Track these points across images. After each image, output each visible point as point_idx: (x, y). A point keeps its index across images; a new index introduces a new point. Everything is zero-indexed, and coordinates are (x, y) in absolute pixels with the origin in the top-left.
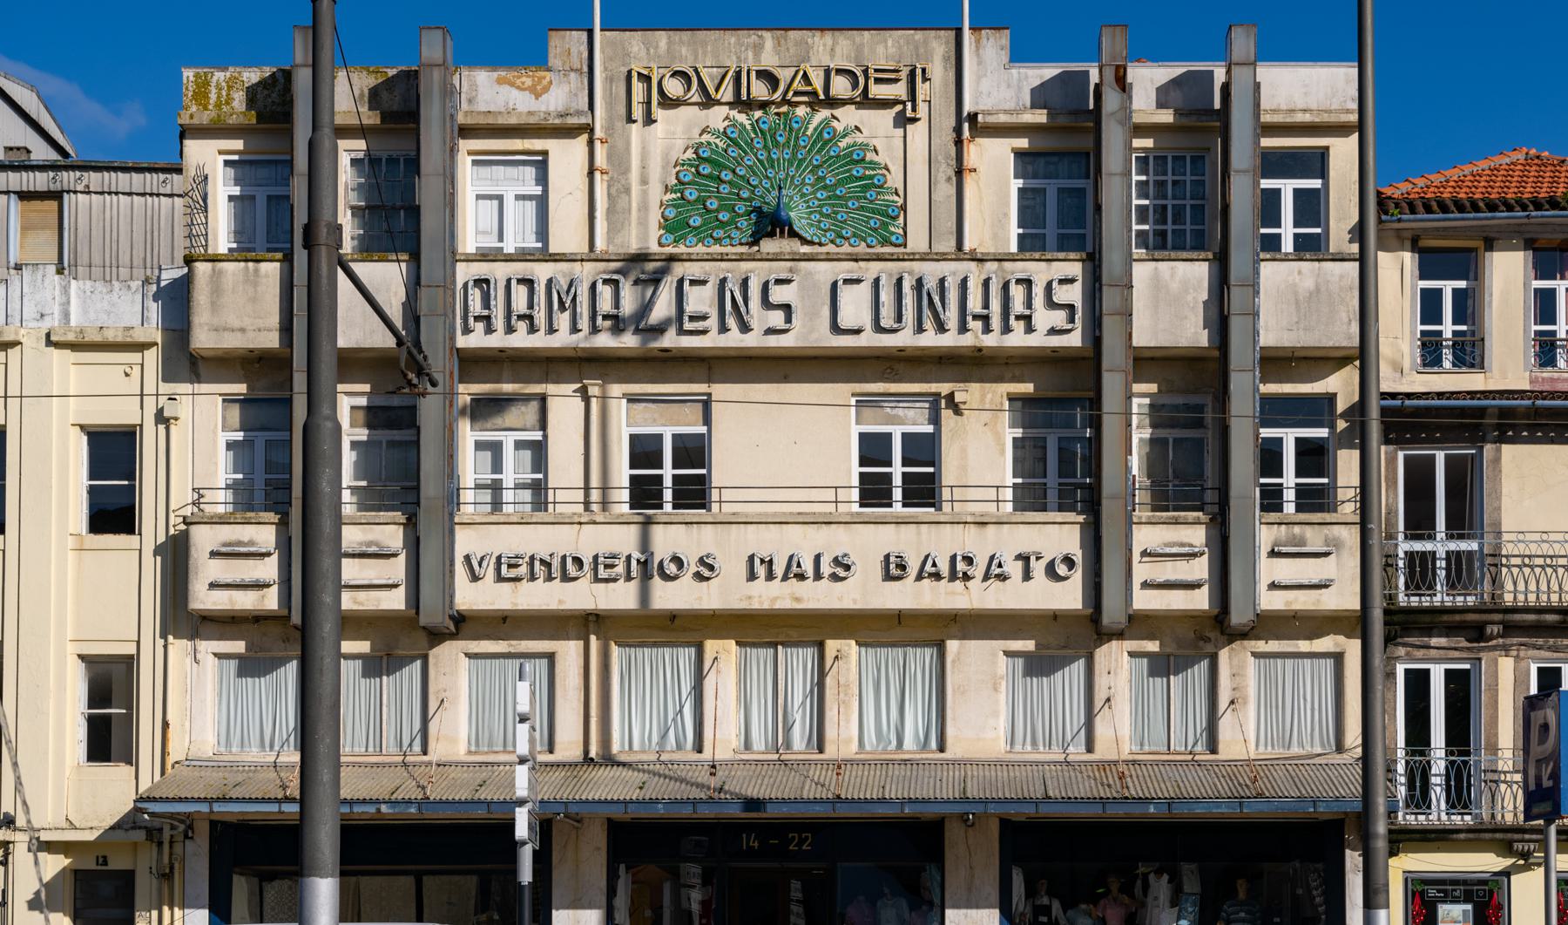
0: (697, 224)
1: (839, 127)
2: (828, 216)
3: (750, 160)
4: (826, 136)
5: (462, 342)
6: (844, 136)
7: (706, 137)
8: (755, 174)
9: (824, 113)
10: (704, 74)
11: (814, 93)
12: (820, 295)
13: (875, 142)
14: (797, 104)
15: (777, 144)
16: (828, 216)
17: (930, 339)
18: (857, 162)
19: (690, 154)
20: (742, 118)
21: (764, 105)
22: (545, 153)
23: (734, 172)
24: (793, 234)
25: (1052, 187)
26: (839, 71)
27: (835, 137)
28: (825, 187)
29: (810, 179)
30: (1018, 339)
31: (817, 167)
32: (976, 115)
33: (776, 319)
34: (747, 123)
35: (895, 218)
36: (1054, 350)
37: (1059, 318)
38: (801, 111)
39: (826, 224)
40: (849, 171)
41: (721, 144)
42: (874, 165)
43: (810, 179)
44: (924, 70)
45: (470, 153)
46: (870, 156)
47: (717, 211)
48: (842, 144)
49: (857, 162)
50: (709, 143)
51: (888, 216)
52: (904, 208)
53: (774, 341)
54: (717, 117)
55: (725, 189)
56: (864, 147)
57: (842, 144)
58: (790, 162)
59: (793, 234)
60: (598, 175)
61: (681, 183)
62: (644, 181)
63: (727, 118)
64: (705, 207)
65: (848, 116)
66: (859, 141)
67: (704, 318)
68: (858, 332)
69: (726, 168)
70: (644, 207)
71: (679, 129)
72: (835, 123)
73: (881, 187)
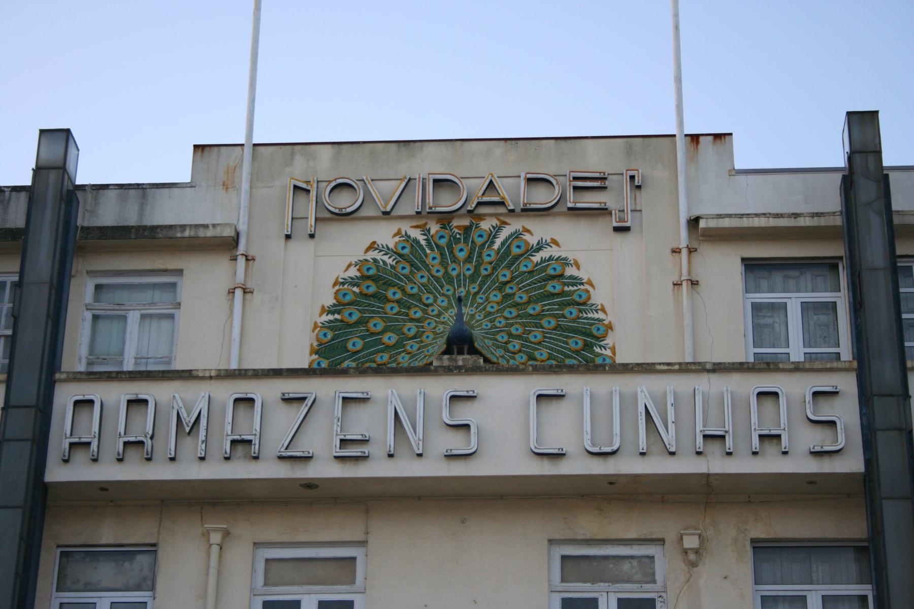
1: (532, 240)
2: (518, 337)
3: (422, 277)
4: (515, 251)
5: (56, 473)
6: (538, 250)
9: (515, 225)
11: (502, 204)
12: (509, 422)
14: (481, 217)
15: (455, 260)
16: (518, 337)
18: (553, 277)
20: (416, 234)
21: (445, 218)
22: (179, 272)
23: (403, 290)
24: (474, 351)
25: (794, 301)
26: (530, 180)
28: (516, 305)
33: (456, 443)
34: (422, 239)
36: (811, 480)
37: (816, 438)
38: (486, 225)
41: (390, 261)
42: (576, 281)
45: (91, 273)
46: (570, 271)
47: (382, 332)
48: (536, 258)
49: (553, 277)
50: (375, 260)
51: (594, 337)
52: (610, 327)
57: (536, 258)
58: (473, 279)
59: (474, 351)
63: (398, 233)
65: (538, 231)
67: (364, 441)
72: (527, 237)
73: (584, 304)
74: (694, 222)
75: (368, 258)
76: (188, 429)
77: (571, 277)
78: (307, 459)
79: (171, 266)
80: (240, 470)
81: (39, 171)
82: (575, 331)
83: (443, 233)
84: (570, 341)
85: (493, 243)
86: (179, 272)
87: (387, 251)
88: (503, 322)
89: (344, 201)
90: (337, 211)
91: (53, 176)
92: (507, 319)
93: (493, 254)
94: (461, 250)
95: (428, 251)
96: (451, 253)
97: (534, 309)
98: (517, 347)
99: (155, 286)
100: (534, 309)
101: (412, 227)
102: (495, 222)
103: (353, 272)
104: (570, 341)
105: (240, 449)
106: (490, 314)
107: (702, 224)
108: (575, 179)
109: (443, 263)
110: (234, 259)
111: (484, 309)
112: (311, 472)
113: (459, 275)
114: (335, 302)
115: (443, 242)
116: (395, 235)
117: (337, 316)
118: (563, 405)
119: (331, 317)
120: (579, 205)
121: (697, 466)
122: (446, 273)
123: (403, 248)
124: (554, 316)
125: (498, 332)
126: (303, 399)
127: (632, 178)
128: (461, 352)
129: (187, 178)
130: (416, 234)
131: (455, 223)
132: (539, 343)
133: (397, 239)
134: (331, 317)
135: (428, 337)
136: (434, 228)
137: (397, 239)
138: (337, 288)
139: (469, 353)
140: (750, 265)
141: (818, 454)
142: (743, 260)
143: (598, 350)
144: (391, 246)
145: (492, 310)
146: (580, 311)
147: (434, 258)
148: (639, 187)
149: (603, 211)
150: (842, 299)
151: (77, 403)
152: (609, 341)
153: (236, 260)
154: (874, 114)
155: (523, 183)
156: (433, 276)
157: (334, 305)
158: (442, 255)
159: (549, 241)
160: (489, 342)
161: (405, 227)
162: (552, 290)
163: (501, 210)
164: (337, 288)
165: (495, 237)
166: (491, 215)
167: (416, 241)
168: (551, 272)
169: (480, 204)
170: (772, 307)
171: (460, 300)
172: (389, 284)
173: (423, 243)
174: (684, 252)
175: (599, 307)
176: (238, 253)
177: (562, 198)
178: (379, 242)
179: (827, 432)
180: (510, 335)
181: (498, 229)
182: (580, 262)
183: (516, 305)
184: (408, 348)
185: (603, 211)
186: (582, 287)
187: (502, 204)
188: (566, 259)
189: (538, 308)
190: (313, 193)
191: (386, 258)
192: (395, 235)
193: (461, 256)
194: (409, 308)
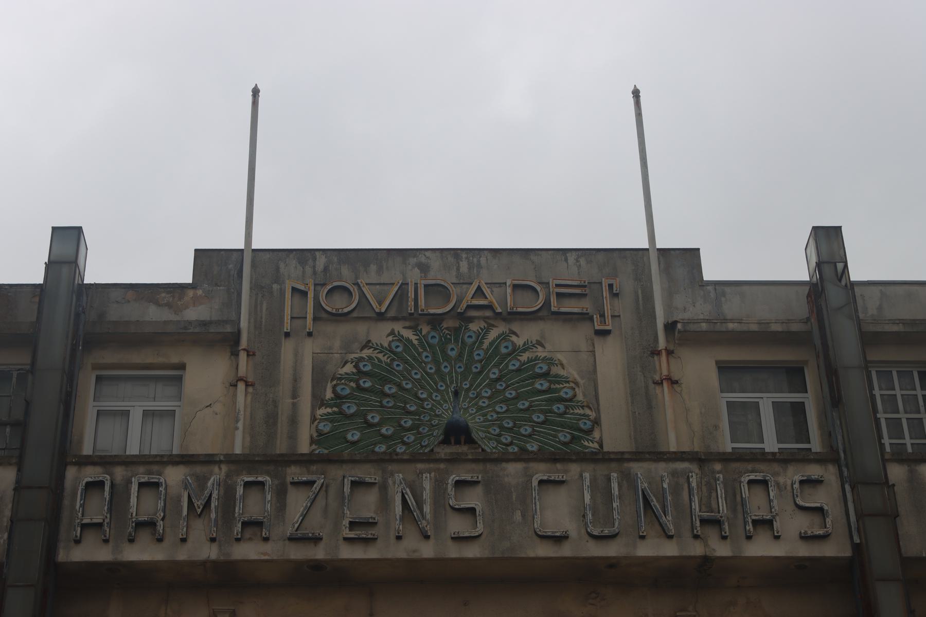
0: (356, 438)
1: (519, 342)
4: (504, 351)
6: (524, 351)
7: (366, 353)
8: (423, 388)
10: (366, 290)
13: (559, 356)
14: (471, 320)
15: (446, 358)
17: (652, 548)
19: (349, 368)
20: (408, 334)
21: (435, 321)
23: (399, 386)
25: (766, 403)
26: (515, 287)
27: (515, 351)
28: (506, 401)
29: (487, 393)
30: (761, 548)
31: (498, 380)
32: (675, 323)
34: (413, 338)
35: (589, 432)
38: (474, 327)
39: (506, 438)
40: (533, 384)
41: (384, 359)
43: (487, 393)
44: (611, 286)
45: (96, 367)
46: (555, 370)
47: (379, 424)
48: (524, 357)
50: (370, 358)
51: (581, 430)
52: (597, 422)
53: (454, 552)
54: (381, 334)
55: (388, 402)
56: (550, 361)
57: (524, 357)
59: (470, 441)
60: (241, 386)
61: (337, 396)
62: (295, 395)
63: (392, 333)
64: (366, 422)
65: (526, 333)
66: (543, 355)
68: (559, 539)
69: (390, 382)
70: (294, 421)
71: (337, 344)
73: (570, 400)
74: (670, 327)
75: (364, 356)
76: (199, 511)
77: (557, 376)
78: (317, 540)
79: (175, 360)
80: (249, 551)
81: (50, 266)
82: (562, 425)
83: (433, 334)
84: (560, 435)
85: (482, 343)
86: (182, 367)
87: (381, 349)
88: (495, 416)
89: (339, 304)
90: (334, 311)
91: (65, 270)
92: (498, 413)
93: (482, 353)
94: (452, 349)
95: (421, 350)
96: (444, 352)
97: (523, 404)
98: (509, 439)
99: (157, 379)
100: (523, 404)
101: (404, 328)
102: (483, 324)
103: (349, 368)
104: (560, 435)
105: (248, 533)
106: (482, 408)
107: (679, 326)
108: (557, 286)
109: (436, 361)
110: (235, 354)
111: (476, 404)
112: (319, 553)
113: (450, 373)
114: (333, 396)
115: (436, 341)
116: (389, 335)
117: (335, 409)
118: (563, 491)
119: (329, 410)
120: (563, 310)
121: (697, 549)
122: (438, 370)
123: (397, 347)
124: (541, 411)
125: (489, 426)
126: (311, 483)
127: (611, 286)
128: (458, 442)
129: (188, 279)
130: (408, 334)
131: (445, 325)
132: (530, 436)
133: (390, 338)
134: (329, 410)
135: (424, 430)
136: (425, 329)
137: (390, 338)
138: (335, 382)
139: (465, 443)
140: (723, 368)
141: (805, 538)
142: (717, 362)
143: (586, 443)
144: (386, 345)
145: (484, 405)
146: (567, 407)
147: (427, 357)
148: (617, 295)
149: (585, 317)
150: (810, 401)
151: (89, 485)
152: (596, 434)
153: (237, 355)
154: (838, 229)
155: (509, 290)
156: (427, 373)
157: (332, 399)
158: (434, 354)
159: (534, 342)
160: (482, 435)
161: (398, 327)
162: (539, 387)
163: (488, 313)
164: (335, 382)
165: (483, 338)
166: (478, 318)
167: (408, 340)
168: (537, 370)
169: (469, 307)
170: (744, 405)
171: (456, 394)
172: (385, 381)
173: (416, 342)
174: (664, 353)
175: (585, 404)
176: (240, 348)
177: (547, 303)
178: (374, 341)
179: (817, 519)
180: (501, 427)
181: (487, 330)
182: (564, 362)
183: (506, 401)
184: (405, 439)
185: (585, 317)
186: (567, 385)
187: (490, 307)
188: (551, 359)
189: (527, 404)
190: (311, 295)
191: (380, 356)
192: (389, 335)
193: (453, 354)
194: (406, 403)
